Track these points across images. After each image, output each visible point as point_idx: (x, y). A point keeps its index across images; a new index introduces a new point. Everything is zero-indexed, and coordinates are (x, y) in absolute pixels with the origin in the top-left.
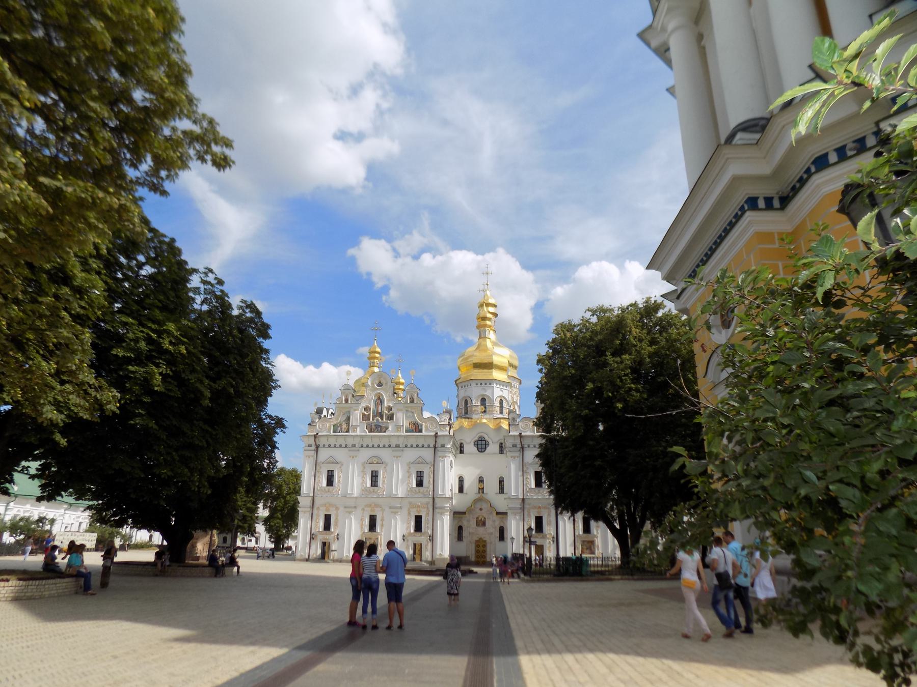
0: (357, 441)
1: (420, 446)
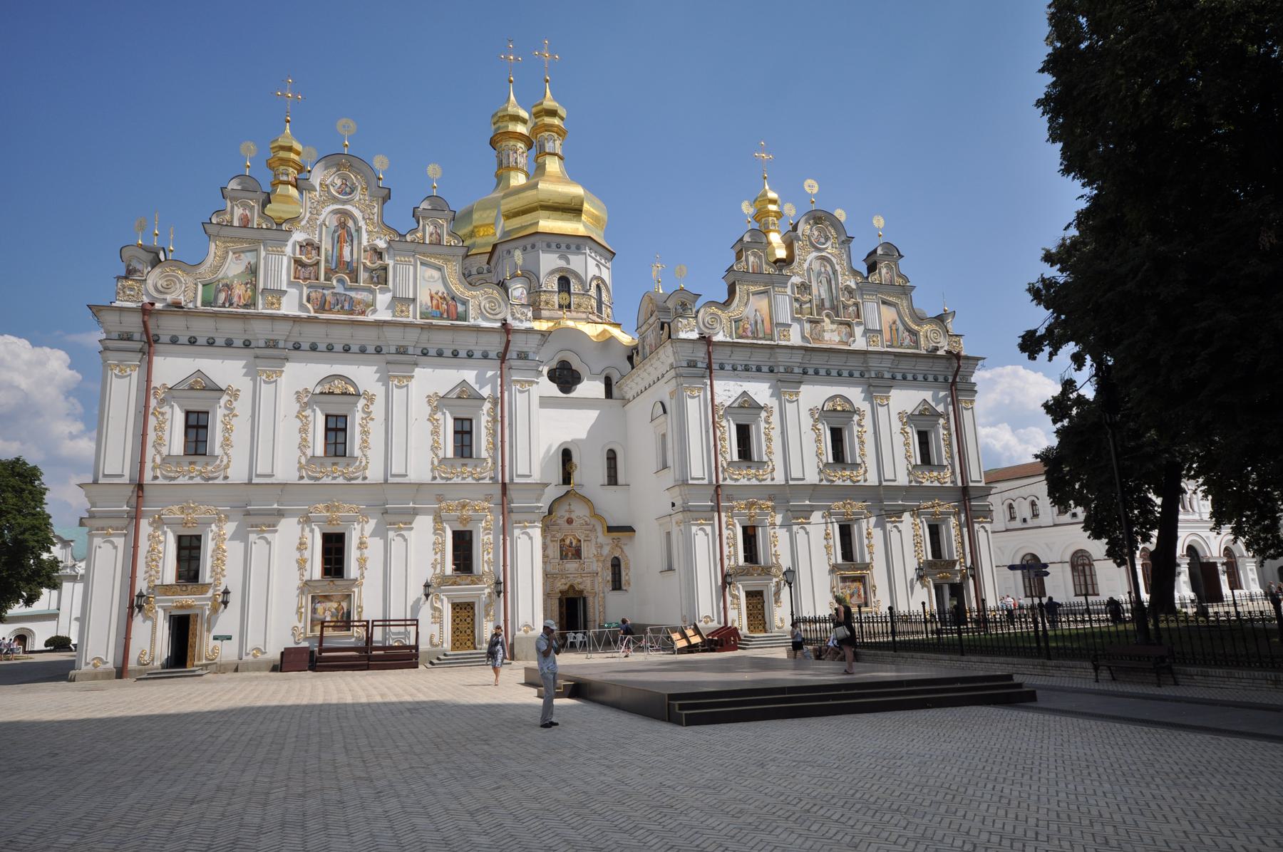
0: (281, 331)
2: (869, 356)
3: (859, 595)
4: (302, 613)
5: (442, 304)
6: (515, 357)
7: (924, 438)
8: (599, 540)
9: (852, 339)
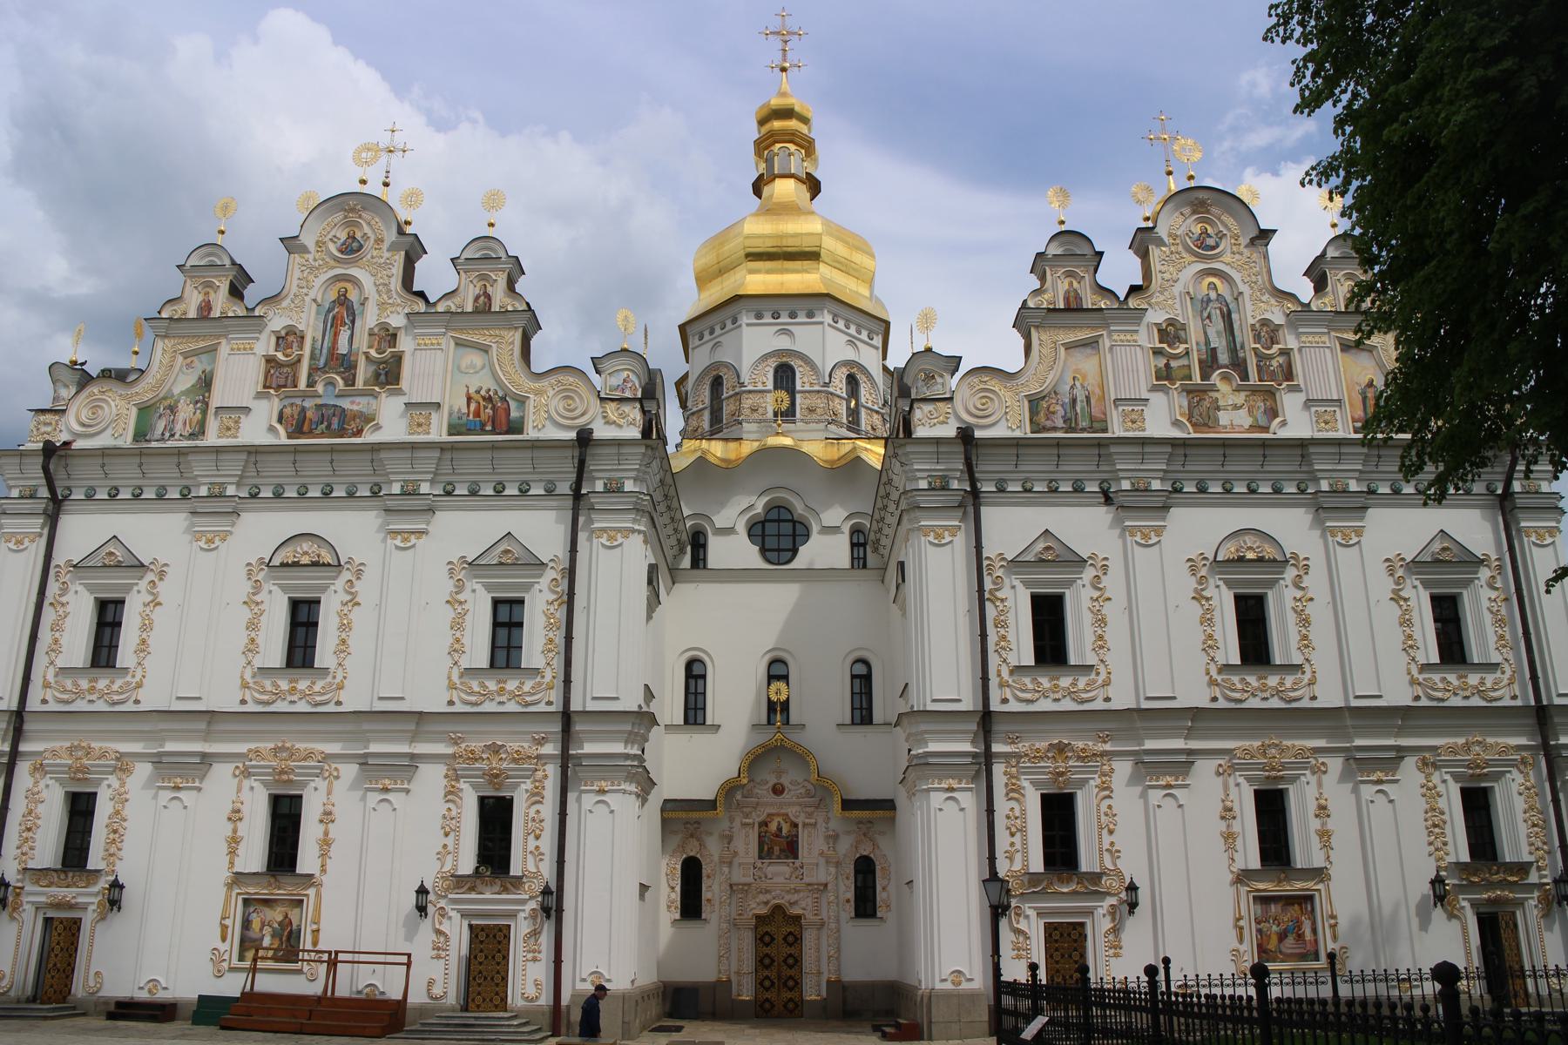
2: (1312, 450)
3: (1300, 937)
4: (227, 927)
5: (485, 408)
6: (599, 486)
7: (1447, 613)
8: (832, 825)
9: (1278, 420)
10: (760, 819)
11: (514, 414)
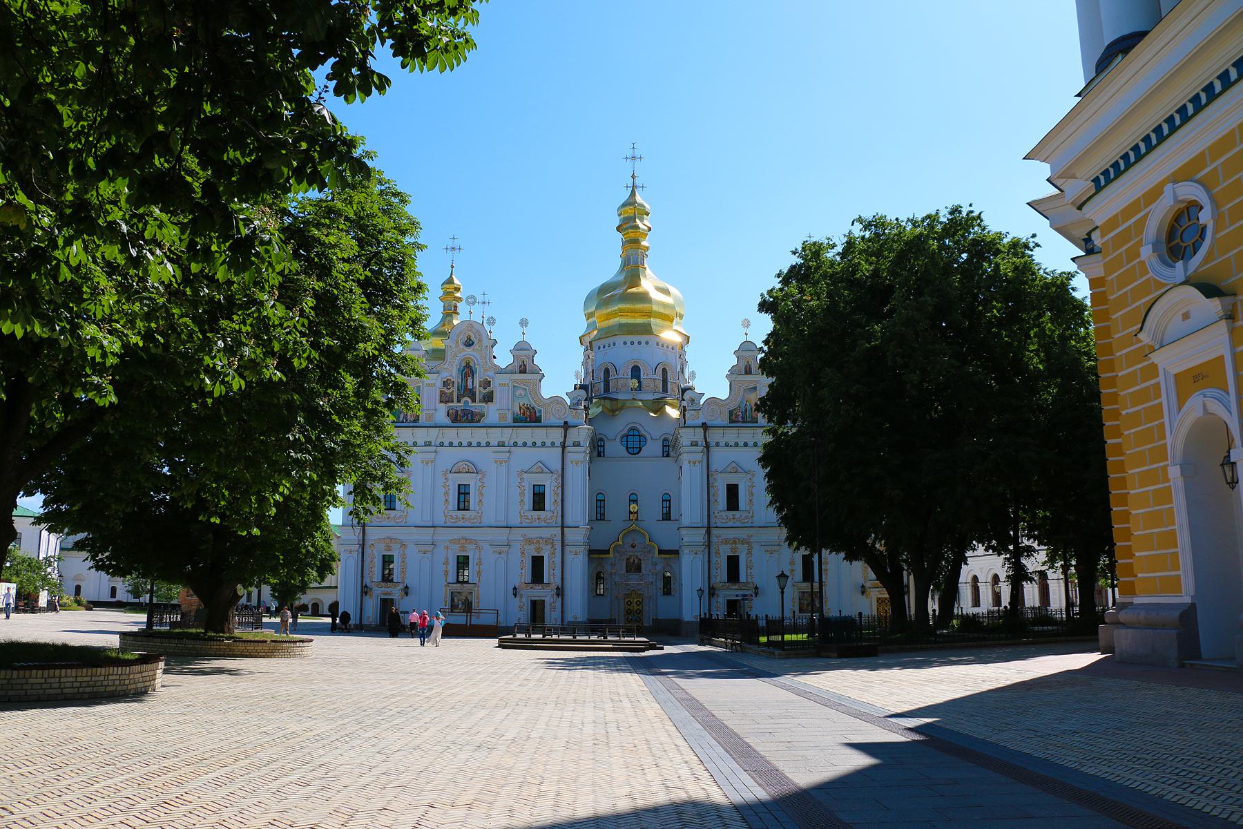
1: (539, 444)
10: (628, 556)
11: (537, 415)
